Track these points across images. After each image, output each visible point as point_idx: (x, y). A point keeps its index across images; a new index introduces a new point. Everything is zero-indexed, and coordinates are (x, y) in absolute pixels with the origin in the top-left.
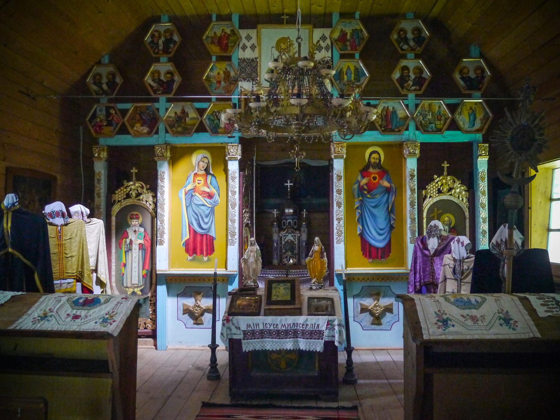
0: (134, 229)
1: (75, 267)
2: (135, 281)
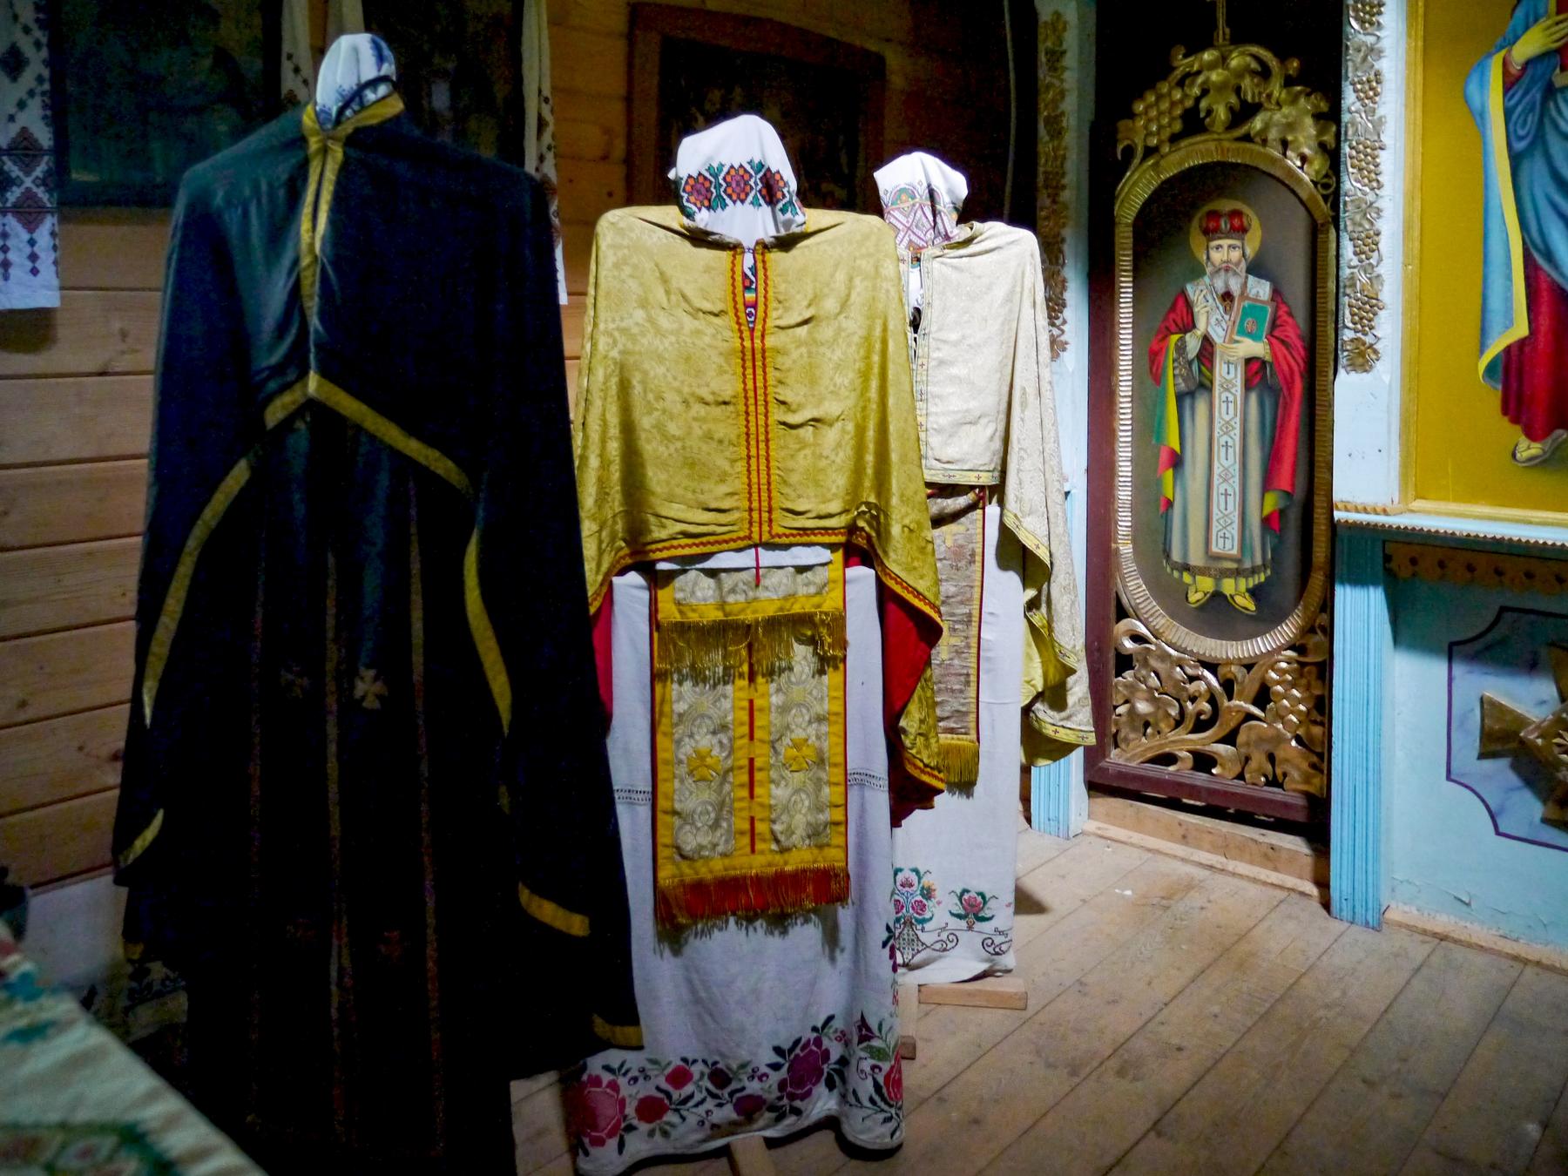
0: (1220, 285)
1: (839, 482)
2: (1227, 542)
